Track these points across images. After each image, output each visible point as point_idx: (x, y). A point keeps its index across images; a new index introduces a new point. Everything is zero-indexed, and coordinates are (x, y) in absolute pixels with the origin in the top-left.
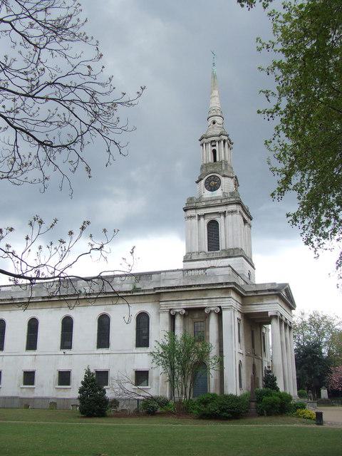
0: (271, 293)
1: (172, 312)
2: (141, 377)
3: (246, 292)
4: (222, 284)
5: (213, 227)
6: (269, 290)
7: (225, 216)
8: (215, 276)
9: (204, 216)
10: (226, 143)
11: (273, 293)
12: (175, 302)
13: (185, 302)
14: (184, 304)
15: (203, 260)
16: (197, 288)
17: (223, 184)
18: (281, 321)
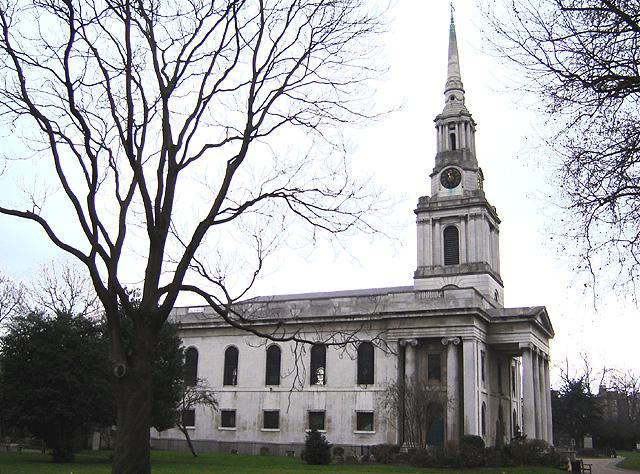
2: (364, 420)
3: (492, 319)
4: (462, 309)
5: (451, 236)
6: (521, 317)
8: (453, 298)
9: (440, 220)
10: (469, 126)
14: (416, 334)
15: (439, 276)
18: (535, 354)
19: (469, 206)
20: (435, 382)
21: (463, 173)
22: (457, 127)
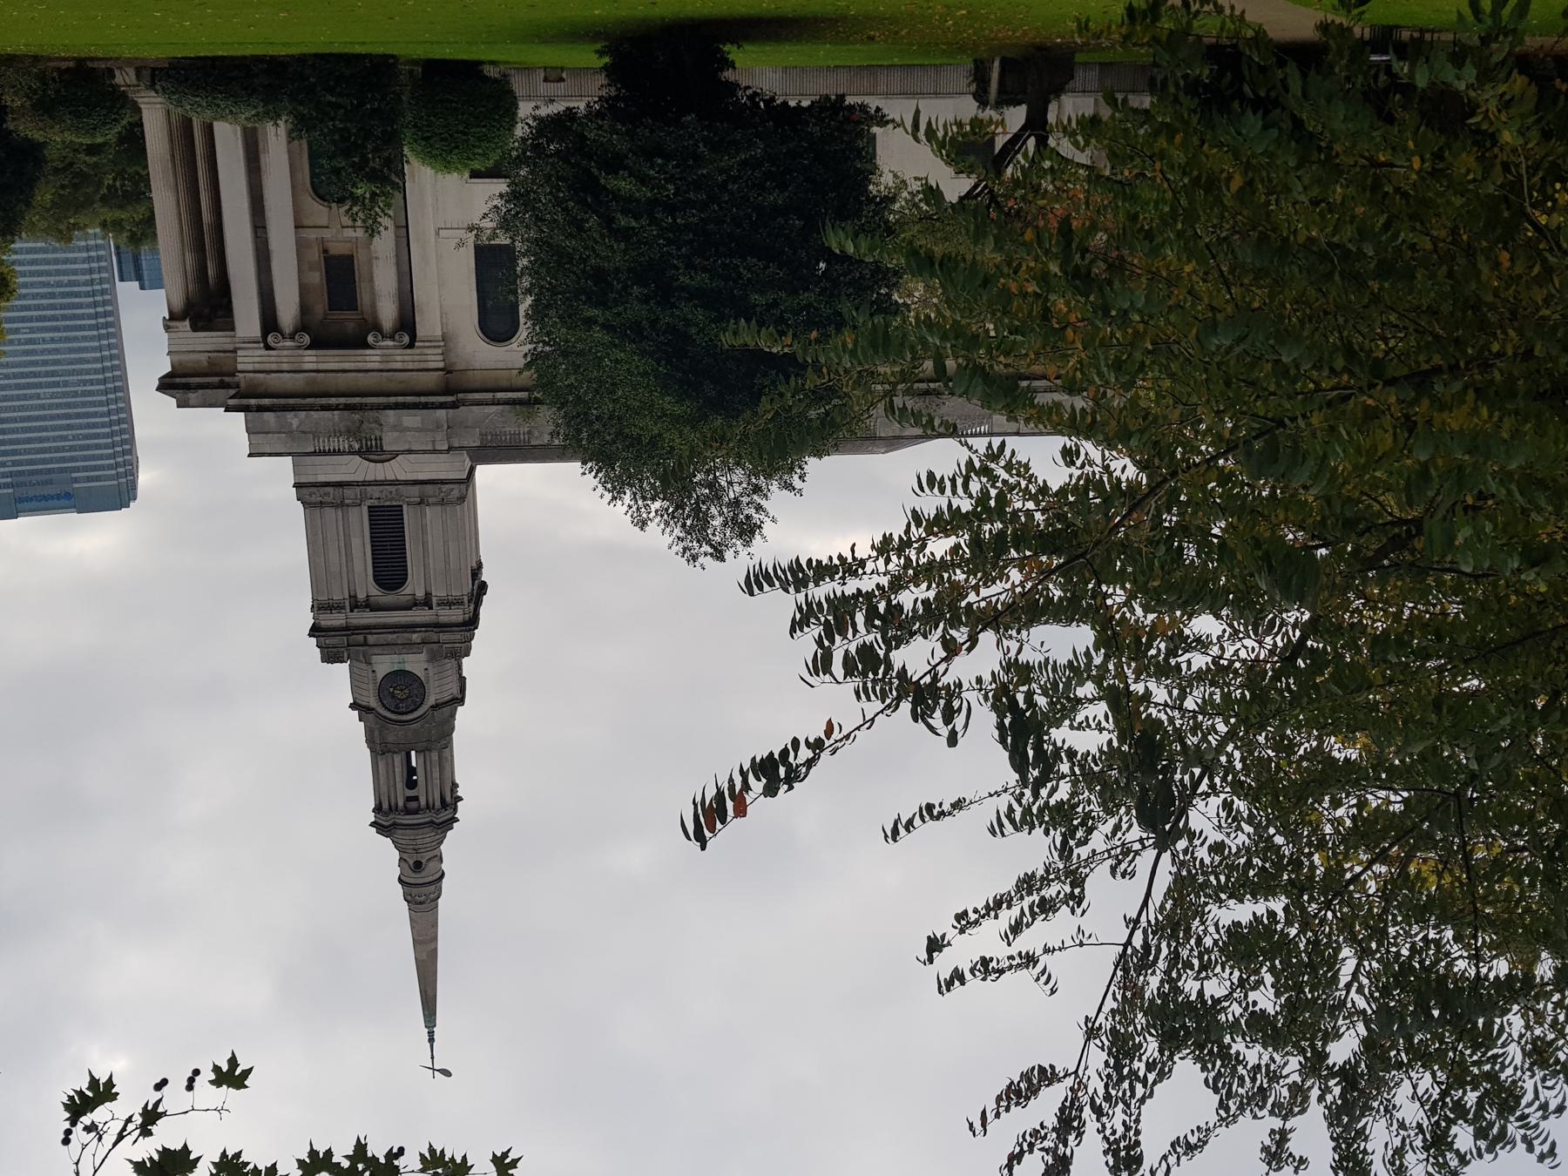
0: (183, 380)
1: (406, 339)
5: (390, 570)
6: (187, 387)
7: (353, 597)
9: (414, 604)
11: (178, 380)
12: (398, 366)
13: (370, 366)
14: (372, 358)
16: (333, 401)
19: (347, 629)
20: (337, 249)
21: (373, 703)
22: (401, 804)
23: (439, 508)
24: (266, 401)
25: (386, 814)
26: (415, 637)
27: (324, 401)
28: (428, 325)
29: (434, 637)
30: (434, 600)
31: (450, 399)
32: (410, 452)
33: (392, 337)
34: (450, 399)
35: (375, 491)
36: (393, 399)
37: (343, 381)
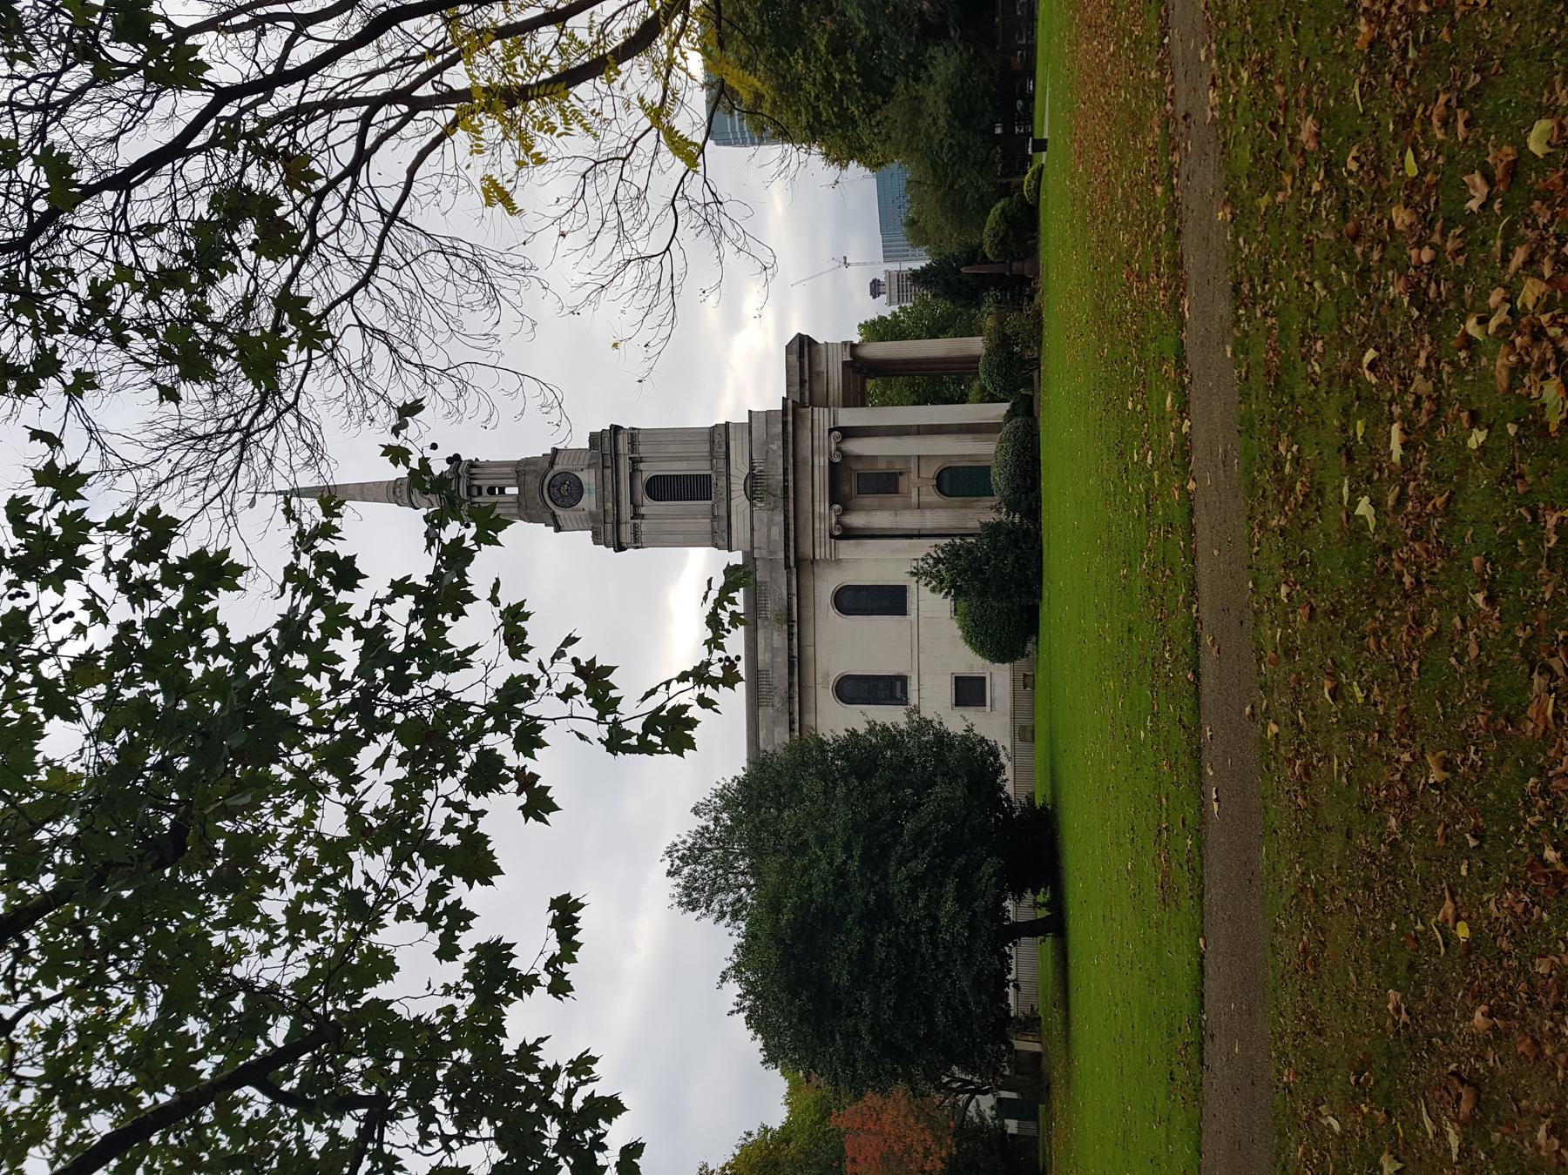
0: (806, 354)
1: (837, 533)
5: (662, 488)
6: (801, 356)
8: (767, 442)
9: (635, 506)
12: (817, 526)
13: (817, 505)
14: (822, 506)
16: (791, 478)
17: (569, 468)
19: (616, 455)
20: (903, 481)
21: (557, 468)
22: (476, 482)
23: (709, 529)
24: (790, 428)
25: (468, 472)
26: (609, 505)
27: (790, 471)
28: (847, 549)
29: (609, 520)
30: (638, 521)
31: (792, 564)
32: (752, 530)
33: (838, 522)
34: (792, 564)
35: (722, 483)
36: (792, 521)
37: (805, 485)
